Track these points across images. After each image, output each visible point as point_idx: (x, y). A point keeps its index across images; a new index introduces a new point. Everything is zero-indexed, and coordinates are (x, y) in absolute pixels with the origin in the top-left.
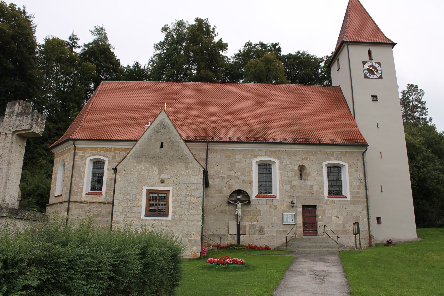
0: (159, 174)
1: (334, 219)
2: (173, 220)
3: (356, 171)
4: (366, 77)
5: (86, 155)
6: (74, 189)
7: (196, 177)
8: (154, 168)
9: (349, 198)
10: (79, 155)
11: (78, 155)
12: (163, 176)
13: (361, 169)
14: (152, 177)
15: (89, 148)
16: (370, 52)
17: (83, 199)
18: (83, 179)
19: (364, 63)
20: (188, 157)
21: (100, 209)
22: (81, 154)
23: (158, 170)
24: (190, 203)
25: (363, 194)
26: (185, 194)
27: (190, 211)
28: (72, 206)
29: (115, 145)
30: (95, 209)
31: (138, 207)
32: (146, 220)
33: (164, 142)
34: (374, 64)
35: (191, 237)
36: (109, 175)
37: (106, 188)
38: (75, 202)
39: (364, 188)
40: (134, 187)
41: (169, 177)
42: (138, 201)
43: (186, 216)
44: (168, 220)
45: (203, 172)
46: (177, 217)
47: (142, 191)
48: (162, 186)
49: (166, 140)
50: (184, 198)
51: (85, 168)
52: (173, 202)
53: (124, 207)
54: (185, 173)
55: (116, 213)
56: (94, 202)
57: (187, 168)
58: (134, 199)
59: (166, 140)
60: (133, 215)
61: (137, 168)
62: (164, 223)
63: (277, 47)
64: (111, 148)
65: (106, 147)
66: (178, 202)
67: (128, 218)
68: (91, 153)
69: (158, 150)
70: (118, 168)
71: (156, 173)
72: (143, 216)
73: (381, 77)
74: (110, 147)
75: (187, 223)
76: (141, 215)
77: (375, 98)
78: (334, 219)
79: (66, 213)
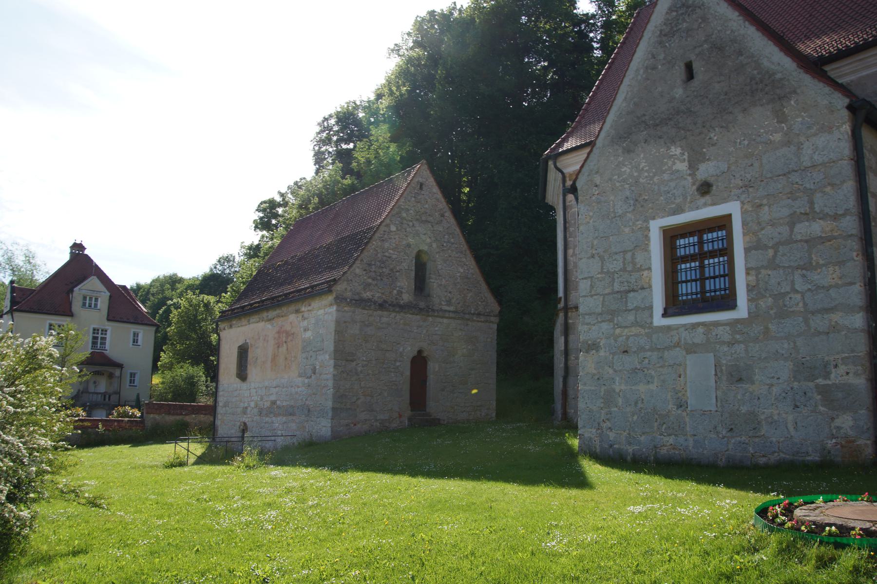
2: (753, 316)
7: (821, 140)
8: (676, 151)
12: (705, 170)
14: (672, 184)
20: (779, 76)
23: (686, 157)
24: (811, 242)
26: (786, 212)
27: (815, 276)
31: (643, 288)
32: (669, 328)
33: (693, 57)
35: (827, 376)
40: (627, 230)
41: (724, 166)
42: (640, 269)
43: (798, 296)
44: (737, 321)
45: (845, 113)
46: (766, 303)
47: (647, 238)
48: (705, 205)
49: (697, 50)
50: (785, 230)
52: (747, 250)
53: (604, 295)
54: (777, 137)
55: (588, 319)
57: (781, 118)
58: (629, 268)
59: (697, 50)
60: (631, 317)
61: (626, 169)
66: (766, 247)
67: (618, 331)
70: (579, 185)
71: (682, 167)
72: (658, 320)
75: (806, 321)
76: (651, 316)
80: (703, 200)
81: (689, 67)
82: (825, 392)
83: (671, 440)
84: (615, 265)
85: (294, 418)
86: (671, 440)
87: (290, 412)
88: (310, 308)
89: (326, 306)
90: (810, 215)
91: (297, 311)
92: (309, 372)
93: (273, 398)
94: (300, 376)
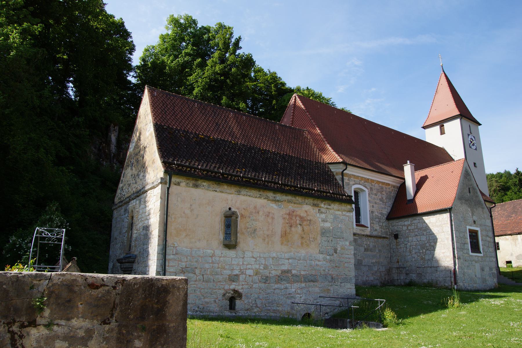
4: (470, 147)
12: (475, 218)
15: (353, 175)
19: (469, 135)
29: (371, 176)
34: (473, 138)
52: (482, 240)
64: (368, 179)
68: (354, 181)
69: (468, 194)
71: (471, 214)
73: (476, 149)
74: (368, 177)
77: (475, 164)
83: (475, 285)
85: (316, 284)
86: (475, 285)
87: (311, 279)
88: (329, 207)
89: (344, 210)
91: (315, 205)
92: (332, 252)
93: (285, 268)
94: (321, 253)
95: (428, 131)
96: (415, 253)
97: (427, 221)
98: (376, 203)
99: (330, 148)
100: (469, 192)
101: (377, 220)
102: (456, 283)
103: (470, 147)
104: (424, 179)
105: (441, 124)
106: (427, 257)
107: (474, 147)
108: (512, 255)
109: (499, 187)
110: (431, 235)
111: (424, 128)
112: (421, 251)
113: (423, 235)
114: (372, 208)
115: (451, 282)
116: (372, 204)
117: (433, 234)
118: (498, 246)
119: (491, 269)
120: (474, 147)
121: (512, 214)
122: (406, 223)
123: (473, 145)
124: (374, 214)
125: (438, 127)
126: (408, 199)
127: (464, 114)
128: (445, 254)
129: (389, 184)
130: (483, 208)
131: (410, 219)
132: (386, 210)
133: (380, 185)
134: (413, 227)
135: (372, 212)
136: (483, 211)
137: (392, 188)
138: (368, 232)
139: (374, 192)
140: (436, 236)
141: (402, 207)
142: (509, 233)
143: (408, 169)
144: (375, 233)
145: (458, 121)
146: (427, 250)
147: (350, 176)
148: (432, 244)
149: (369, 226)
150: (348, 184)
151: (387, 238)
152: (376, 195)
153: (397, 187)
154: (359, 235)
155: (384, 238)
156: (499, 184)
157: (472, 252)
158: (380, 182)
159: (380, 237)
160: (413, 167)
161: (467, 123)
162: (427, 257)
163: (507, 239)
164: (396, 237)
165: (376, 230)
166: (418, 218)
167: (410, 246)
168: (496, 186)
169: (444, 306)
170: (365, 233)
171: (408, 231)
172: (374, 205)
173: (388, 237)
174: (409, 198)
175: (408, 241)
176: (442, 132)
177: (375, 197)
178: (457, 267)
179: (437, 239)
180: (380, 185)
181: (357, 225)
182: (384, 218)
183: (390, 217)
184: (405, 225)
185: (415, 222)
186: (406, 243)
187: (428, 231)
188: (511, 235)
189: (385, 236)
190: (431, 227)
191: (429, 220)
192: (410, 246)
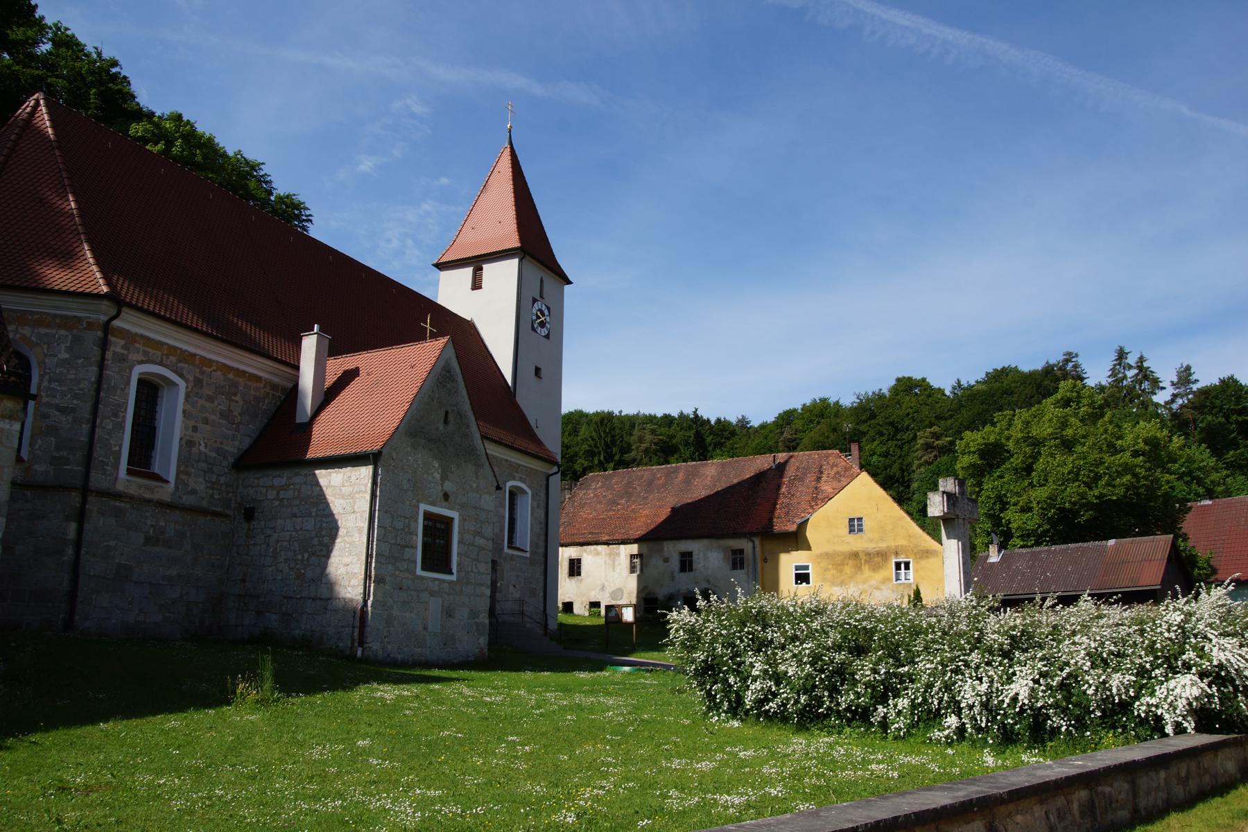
0: (444, 477)
1: (511, 588)
3: (538, 507)
4: (534, 329)
5: (134, 357)
6: (98, 452)
9: (528, 555)
10: (115, 353)
11: (112, 348)
12: (449, 486)
13: (542, 504)
15: (142, 337)
16: (542, 281)
17: (120, 487)
18: (121, 426)
19: (535, 301)
21: (162, 524)
22: (119, 350)
25: (541, 550)
28: (93, 504)
30: (149, 522)
36: (186, 428)
37: (178, 467)
38: (102, 493)
39: (543, 538)
42: (411, 534)
51: (128, 394)
56: (149, 501)
60: (405, 566)
62: (445, 586)
63: (114, 70)
64: (194, 355)
65: (184, 347)
68: (145, 353)
69: (441, 426)
71: (438, 476)
73: (547, 336)
74: (192, 350)
77: (537, 370)
78: (511, 588)
79: (73, 526)
80: (445, 504)
81: (447, 413)
82: (477, 624)
83: (419, 650)
84: (399, 525)
86: (419, 650)
90: (478, 533)
95: (445, 275)
96: (286, 560)
97: (323, 482)
98: (206, 421)
99: (89, 254)
100: (446, 421)
101: (203, 465)
102: (361, 644)
103: (534, 329)
104: (349, 376)
105: (477, 262)
106: (309, 574)
107: (544, 332)
108: (603, 588)
109: (655, 444)
110: (326, 516)
111: (441, 266)
112: (300, 557)
113: (310, 515)
114: (190, 432)
115: (353, 640)
116: (191, 423)
117: (332, 515)
118: (579, 568)
119: (474, 614)
120: (544, 332)
121: (622, 498)
122: (277, 482)
123: (542, 325)
124: (194, 450)
125: (469, 271)
126: (298, 421)
127: (533, 248)
128: (348, 568)
129: (258, 379)
130: (479, 466)
131: (287, 473)
132: (237, 443)
133: (231, 376)
134: (290, 494)
135: (188, 444)
136: (476, 473)
137: (267, 390)
138: (165, 493)
139: (207, 391)
140: (336, 522)
141: (280, 440)
142: (606, 538)
143: (309, 345)
144: (188, 500)
145: (512, 265)
146: (313, 554)
147: (130, 338)
148: (326, 540)
149: (172, 478)
150: (122, 359)
151: (227, 516)
152: (210, 399)
153: (284, 388)
154: (131, 498)
155: (215, 514)
156: (656, 439)
157: (423, 569)
158: (230, 369)
159: (204, 512)
160: (327, 342)
161: (536, 273)
162: (309, 574)
163: (598, 554)
164: (249, 514)
165: (193, 492)
166: (304, 472)
167: (278, 541)
168: (651, 442)
169: (221, 697)
170: (156, 497)
171: (277, 503)
172: (201, 426)
173: (230, 513)
174: (301, 419)
175: (274, 528)
176: (476, 285)
177: (208, 404)
178: (370, 603)
179: (337, 529)
180: (231, 376)
181: (129, 472)
182: (225, 463)
183: (246, 463)
184: (272, 487)
185: (297, 480)
186: (269, 532)
187: (321, 507)
188: (607, 543)
189: (219, 509)
190: (330, 498)
191: (332, 481)
192: (278, 541)
